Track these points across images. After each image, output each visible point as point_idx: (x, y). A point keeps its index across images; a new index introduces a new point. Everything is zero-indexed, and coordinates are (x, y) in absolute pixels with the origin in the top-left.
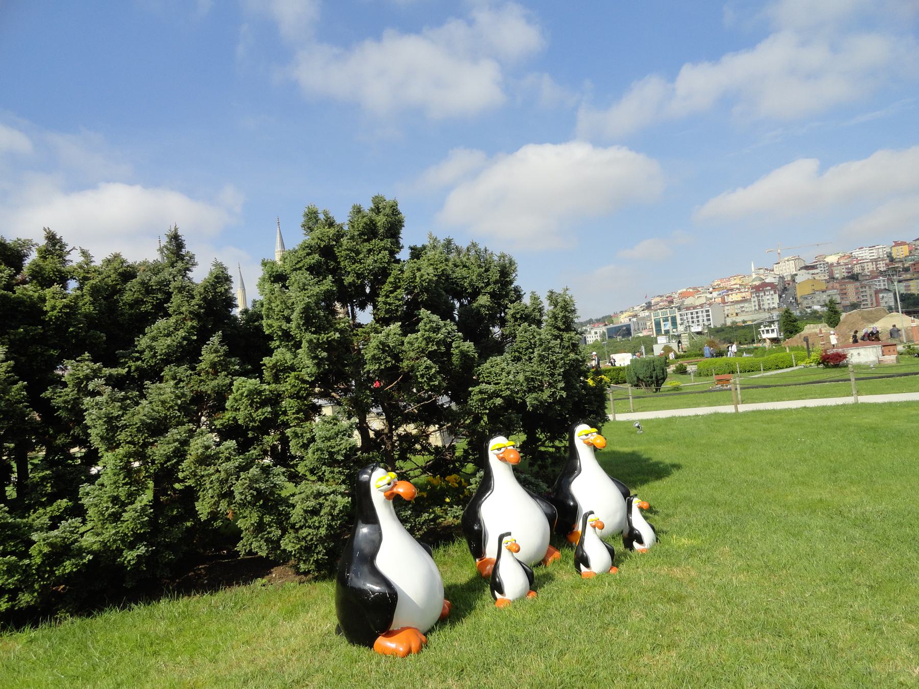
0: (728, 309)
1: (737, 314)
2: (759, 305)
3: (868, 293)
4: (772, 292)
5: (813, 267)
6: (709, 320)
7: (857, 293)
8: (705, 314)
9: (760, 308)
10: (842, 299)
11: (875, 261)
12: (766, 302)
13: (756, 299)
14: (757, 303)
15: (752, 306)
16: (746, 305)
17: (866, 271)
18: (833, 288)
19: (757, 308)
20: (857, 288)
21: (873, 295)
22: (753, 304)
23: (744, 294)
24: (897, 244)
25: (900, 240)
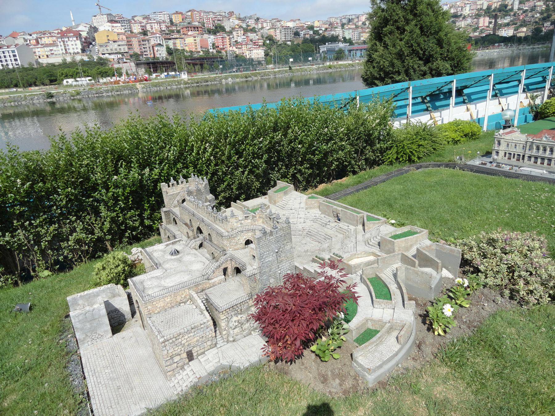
0: (40, 51)
1: (47, 56)
2: (66, 50)
3: (147, 46)
4: (75, 39)
5: (116, 22)
6: (16, 60)
7: (139, 45)
8: (11, 54)
9: (67, 53)
10: (129, 49)
11: (159, 23)
12: (71, 47)
13: (62, 43)
14: (63, 47)
15: (59, 50)
16: (55, 48)
17: (154, 29)
18: (123, 40)
19: (64, 51)
20: (139, 42)
21: (151, 48)
22: (60, 48)
23: (54, 39)
24: (177, 13)
25: (180, 11)
